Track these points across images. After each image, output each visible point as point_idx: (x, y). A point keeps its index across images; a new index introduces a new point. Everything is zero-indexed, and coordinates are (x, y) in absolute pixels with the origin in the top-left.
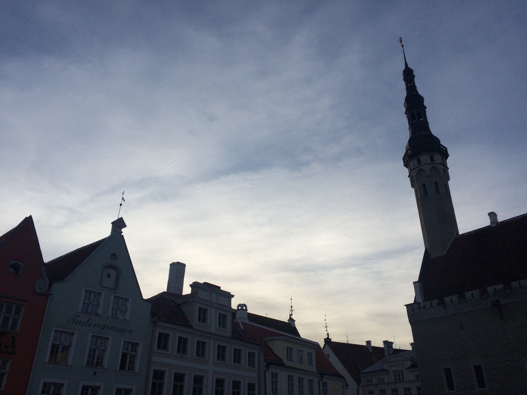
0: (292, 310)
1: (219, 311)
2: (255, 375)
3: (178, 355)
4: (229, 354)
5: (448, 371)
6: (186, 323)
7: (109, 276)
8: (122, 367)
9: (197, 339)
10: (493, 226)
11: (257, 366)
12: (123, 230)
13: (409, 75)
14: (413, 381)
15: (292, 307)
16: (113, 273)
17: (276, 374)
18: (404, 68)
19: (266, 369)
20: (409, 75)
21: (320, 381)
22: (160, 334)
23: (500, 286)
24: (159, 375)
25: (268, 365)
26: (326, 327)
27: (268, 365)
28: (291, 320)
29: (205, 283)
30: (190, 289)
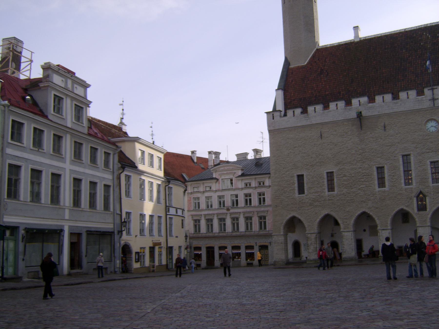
0: (123, 114)
1: (75, 102)
3: (34, 149)
5: (300, 178)
10: (356, 40)
11: (111, 167)
14: (242, 189)
15: (123, 110)
19: (120, 171)
21: (166, 186)
23: (364, 99)
26: (152, 135)
27: (123, 168)
28: (121, 123)
29: (58, 66)
30: (41, 71)
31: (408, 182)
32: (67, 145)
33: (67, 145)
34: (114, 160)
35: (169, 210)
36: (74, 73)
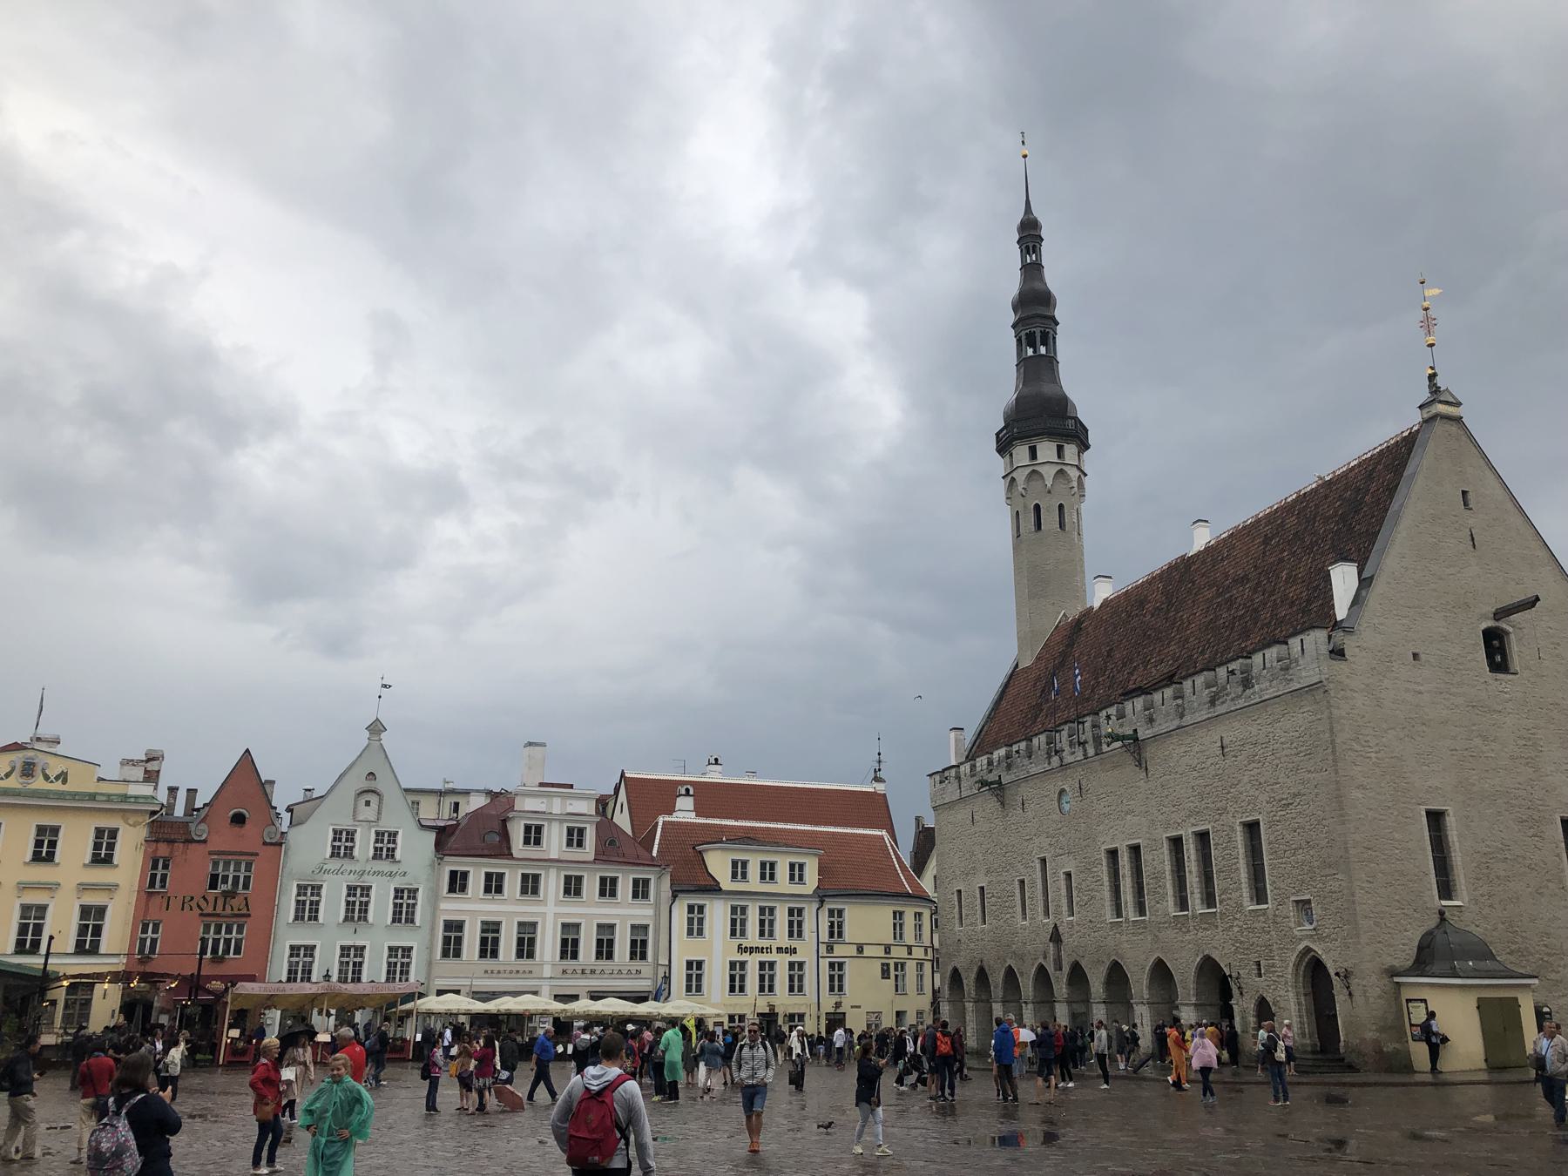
2: (650, 912)
4: (591, 885)
6: (502, 850)
7: (368, 803)
8: (396, 919)
9: (521, 871)
12: (383, 735)
13: (1030, 235)
16: (373, 799)
17: (701, 909)
18: (1020, 215)
20: (1030, 235)
22: (453, 874)
24: (453, 927)
25: (674, 897)
27: (674, 897)
31: (1047, 913)
32: (552, 883)
33: (552, 883)
34: (660, 886)
35: (830, 949)
36: (571, 786)
